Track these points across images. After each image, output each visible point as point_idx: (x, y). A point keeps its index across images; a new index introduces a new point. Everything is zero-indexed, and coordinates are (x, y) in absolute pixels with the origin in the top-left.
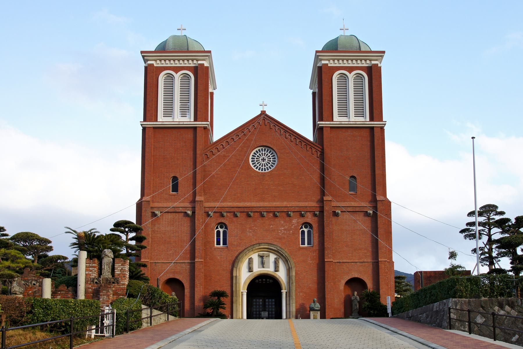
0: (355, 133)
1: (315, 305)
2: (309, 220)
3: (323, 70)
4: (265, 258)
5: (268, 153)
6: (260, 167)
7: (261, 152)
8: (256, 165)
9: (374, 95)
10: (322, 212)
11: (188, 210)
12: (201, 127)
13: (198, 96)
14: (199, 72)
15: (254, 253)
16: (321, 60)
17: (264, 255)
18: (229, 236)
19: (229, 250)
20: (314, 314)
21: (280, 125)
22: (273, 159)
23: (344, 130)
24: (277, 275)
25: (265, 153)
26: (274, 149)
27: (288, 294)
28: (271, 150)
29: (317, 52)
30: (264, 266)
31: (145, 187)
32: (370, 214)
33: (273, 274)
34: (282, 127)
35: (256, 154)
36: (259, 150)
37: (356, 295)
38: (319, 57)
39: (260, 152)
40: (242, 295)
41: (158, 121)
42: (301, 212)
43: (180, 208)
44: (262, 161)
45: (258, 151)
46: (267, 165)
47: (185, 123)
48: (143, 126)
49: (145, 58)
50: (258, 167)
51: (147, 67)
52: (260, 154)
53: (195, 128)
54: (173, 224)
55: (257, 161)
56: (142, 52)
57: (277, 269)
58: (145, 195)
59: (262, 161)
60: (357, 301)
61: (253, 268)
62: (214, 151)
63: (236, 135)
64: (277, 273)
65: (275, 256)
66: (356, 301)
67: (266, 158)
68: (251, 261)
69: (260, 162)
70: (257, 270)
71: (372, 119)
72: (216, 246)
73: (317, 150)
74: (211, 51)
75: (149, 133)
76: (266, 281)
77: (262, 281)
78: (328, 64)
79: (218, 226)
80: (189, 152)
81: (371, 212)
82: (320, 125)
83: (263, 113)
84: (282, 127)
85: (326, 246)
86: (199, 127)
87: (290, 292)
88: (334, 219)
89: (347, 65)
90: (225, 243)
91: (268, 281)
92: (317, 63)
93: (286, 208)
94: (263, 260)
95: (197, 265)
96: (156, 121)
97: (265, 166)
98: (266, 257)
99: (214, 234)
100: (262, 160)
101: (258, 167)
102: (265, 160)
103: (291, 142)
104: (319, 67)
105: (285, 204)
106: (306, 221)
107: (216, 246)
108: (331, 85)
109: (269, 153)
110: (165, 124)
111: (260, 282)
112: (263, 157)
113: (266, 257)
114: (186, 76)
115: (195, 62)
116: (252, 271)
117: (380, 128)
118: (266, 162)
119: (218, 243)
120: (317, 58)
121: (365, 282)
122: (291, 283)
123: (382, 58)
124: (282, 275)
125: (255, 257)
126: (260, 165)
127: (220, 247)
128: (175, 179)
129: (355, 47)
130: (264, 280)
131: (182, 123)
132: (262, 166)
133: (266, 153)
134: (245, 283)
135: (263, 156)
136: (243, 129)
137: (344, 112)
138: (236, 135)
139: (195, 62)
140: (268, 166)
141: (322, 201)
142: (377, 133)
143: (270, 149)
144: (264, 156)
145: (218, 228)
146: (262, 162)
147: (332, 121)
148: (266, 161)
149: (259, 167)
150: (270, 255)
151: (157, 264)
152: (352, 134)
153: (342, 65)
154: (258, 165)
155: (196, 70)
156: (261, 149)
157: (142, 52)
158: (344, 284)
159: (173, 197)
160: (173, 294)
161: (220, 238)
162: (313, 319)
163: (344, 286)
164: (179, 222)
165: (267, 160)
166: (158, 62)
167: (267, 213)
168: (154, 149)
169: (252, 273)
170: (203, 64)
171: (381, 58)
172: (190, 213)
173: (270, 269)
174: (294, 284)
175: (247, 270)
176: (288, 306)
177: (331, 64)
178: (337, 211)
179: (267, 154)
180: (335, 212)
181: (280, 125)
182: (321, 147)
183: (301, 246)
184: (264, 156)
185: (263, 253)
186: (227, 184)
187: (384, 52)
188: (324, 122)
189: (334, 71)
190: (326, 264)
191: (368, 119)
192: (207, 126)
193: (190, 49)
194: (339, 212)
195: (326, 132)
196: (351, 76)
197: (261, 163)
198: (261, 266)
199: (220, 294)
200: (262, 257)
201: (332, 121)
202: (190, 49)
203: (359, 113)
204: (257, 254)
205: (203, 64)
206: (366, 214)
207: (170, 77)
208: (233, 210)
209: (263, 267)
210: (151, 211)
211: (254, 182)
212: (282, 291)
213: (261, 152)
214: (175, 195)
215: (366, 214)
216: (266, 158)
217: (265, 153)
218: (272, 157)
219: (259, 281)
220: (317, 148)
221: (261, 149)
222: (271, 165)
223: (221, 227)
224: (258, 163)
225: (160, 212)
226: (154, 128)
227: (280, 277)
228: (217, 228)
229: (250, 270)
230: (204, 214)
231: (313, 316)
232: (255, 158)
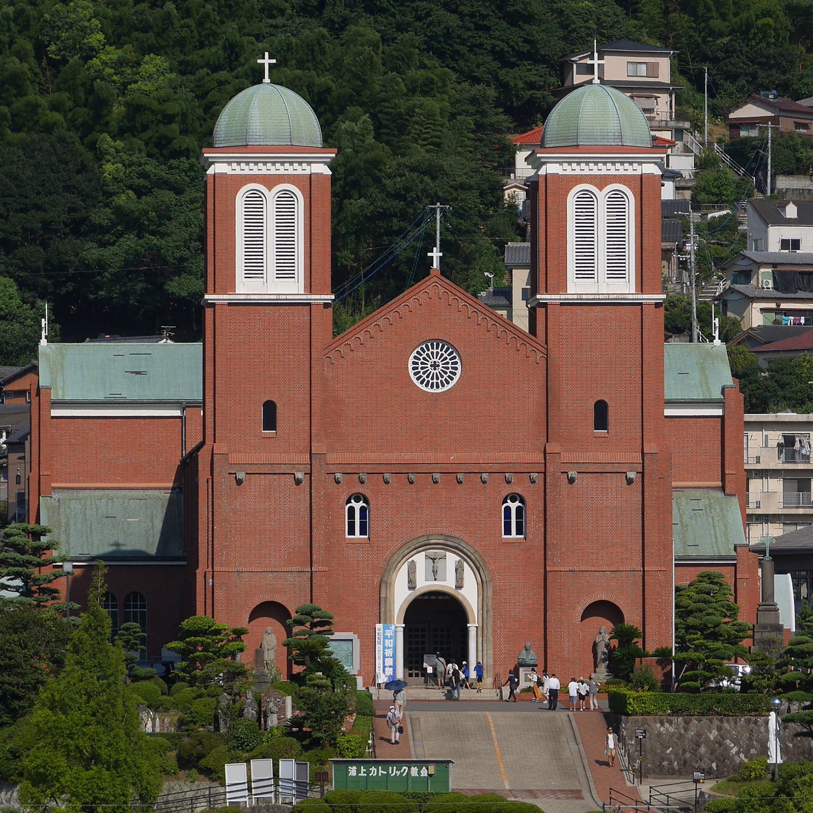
6: (428, 381)
47: (288, 297)
50: (424, 379)
57: (459, 587)
61: (415, 581)
65: (458, 558)
70: (424, 584)
124: (470, 595)
131: (284, 297)
146: (433, 371)
149: (427, 379)
154: (425, 376)
173: (447, 583)
209: (435, 580)
212: (468, 625)
229: (412, 586)
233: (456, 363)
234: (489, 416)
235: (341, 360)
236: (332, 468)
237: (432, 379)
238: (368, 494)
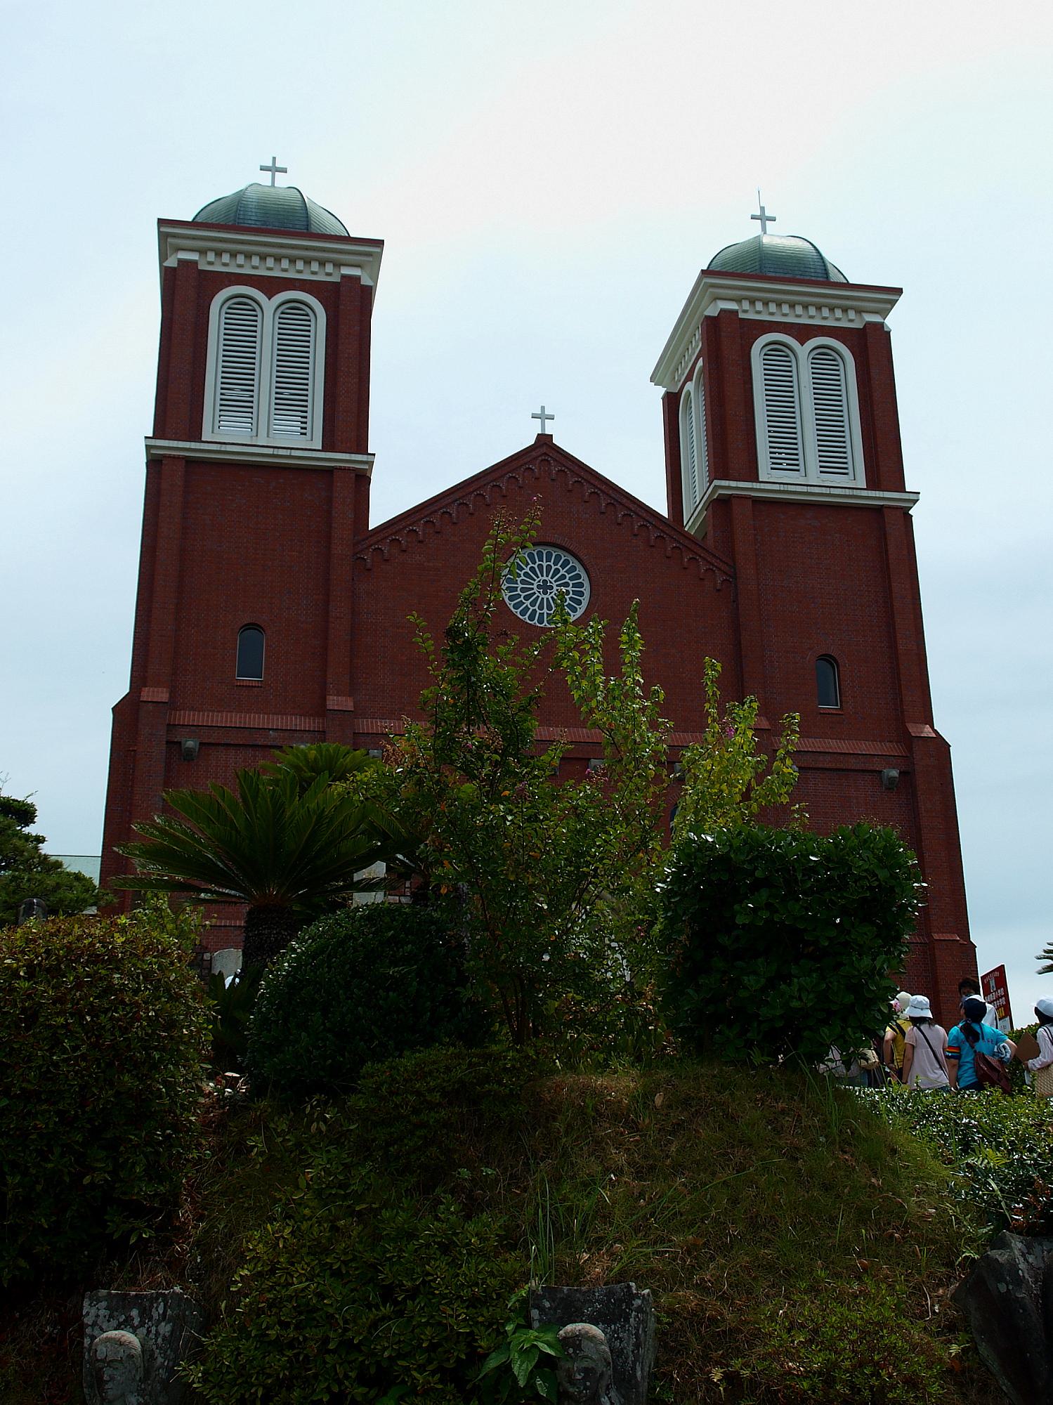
7: (538, 563)
29: (702, 270)
34: (603, 488)
47: (294, 453)
48: (153, 451)
51: (175, 268)
53: (329, 472)
55: (523, 590)
56: (161, 222)
67: (553, 581)
71: (873, 483)
78: (736, 312)
82: (721, 492)
83: (544, 441)
89: (791, 319)
101: (527, 608)
104: (708, 318)
126: (533, 604)
129: (812, 270)
131: (287, 452)
133: (554, 568)
137: (789, 458)
139: (329, 268)
143: (566, 554)
144: (547, 576)
147: (756, 480)
153: (778, 318)
157: (161, 222)
177: (749, 312)
179: (557, 571)
184: (547, 576)
187: (899, 291)
192: (366, 467)
201: (756, 480)
202: (314, 229)
203: (832, 460)
205: (358, 278)
213: (538, 563)
216: (553, 581)
233: (581, 585)
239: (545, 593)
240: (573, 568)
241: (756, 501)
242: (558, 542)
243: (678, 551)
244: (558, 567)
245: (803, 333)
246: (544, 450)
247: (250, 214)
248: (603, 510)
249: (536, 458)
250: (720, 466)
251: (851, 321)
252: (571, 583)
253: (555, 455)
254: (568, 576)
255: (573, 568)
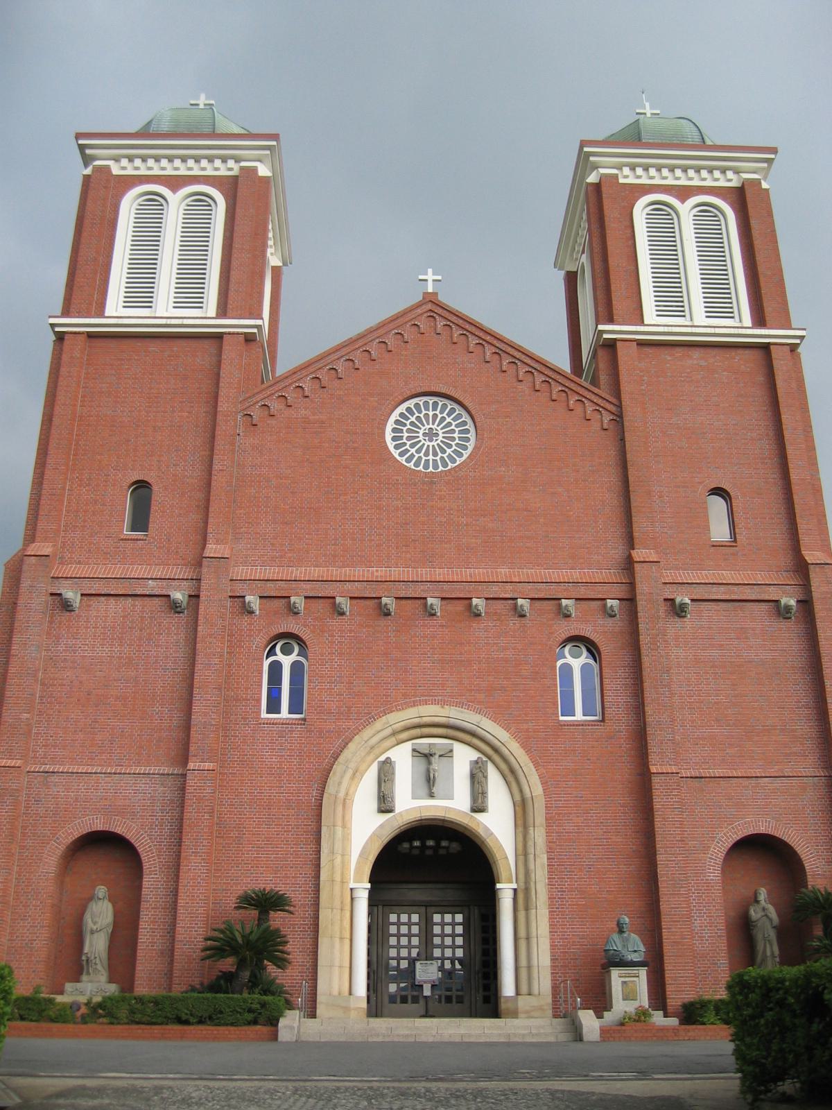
0: (711, 360)
1: (625, 941)
2: (587, 631)
3: (604, 189)
4: (435, 760)
5: (445, 415)
6: (420, 458)
7: (424, 412)
8: (407, 451)
9: (760, 258)
10: (630, 601)
11: (178, 589)
12: (238, 334)
13: (234, 250)
14: (242, 192)
15: (398, 744)
16: (595, 167)
17: (433, 751)
18: (310, 681)
19: (310, 731)
20: (627, 979)
21: (481, 334)
22: (460, 432)
23: (679, 352)
24: (479, 823)
25: (435, 416)
26: (466, 403)
27: (523, 898)
28: (456, 406)
30: (434, 790)
31: (41, 513)
32: (788, 609)
33: (465, 821)
34: (488, 338)
35: (408, 419)
36: (417, 405)
37: (763, 902)
38: (592, 159)
39: (420, 412)
40: (352, 899)
41: (106, 315)
42: (560, 599)
43: (150, 582)
44: (427, 438)
45: (414, 409)
46: (443, 451)
48: (57, 329)
49: (88, 152)
50: (412, 456)
52: (418, 418)
53: (219, 337)
54: (122, 637)
55: (409, 438)
56: (78, 136)
58: (38, 539)
59: (427, 438)
60: (772, 924)
62: (275, 406)
63: (377, 341)
64: (478, 816)
65: (474, 755)
66: (769, 927)
67: (438, 428)
68: (386, 773)
69: (420, 441)
71: (760, 319)
72: (264, 715)
73: (600, 406)
74: (278, 135)
75: (74, 350)
76: (438, 846)
77: (423, 847)
79: (274, 646)
80: (193, 407)
81: (793, 602)
82: (605, 336)
84: (488, 338)
85: (649, 720)
86: (229, 333)
87: (527, 890)
88: (674, 627)
90: (295, 707)
91: (444, 847)
92: (585, 174)
93: (509, 586)
94: (431, 767)
95: (191, 781)
96: (101, 314)
97: (435, 454)
98: (440, 756)
99: (261, 673)
100: (424, 434)
101: (412, 456)
102: (437, 435)
103: (519, 383)
105: (503, 572)
106: (577, 633)
107: (264, 715)
108: (629, 231)
109: (449, 415)
110: (172, 323)
111: (416, 852)
112: (429, 427)
113: (440, 756)
114: (202, 200)
115: (231, 163)
116: (390, 811)
117: (788, 347)
118: (439, 442)
119: (274, 706)
120: (584, 162)
121: (795, 853)
122: (531, 857)
123: (770, 167)
125: (402, 757)
126: (418, 451)
127: (278, 721)
128: (141, 487)
130: (431, 843)
132: (427, 454)
133: (440, 416)
134: (363, 854)
135: (428, 424)
136: (366, 344)
137: (673, 300)
138: (377, 341)
140: (447, 454)
141: (629, 565)
142: (780, 362)
143: (452, 403)
144: (433, 424)
145: (276, 655)
146: (427, 443)
147: (642, 323)
148: (440, 438)
149: (417, 456)
150: (455, 753)
151: (54, 778)
152: (703, 363)
153: (657, 181)
154: (413, 451)
155: (231, 187)
156: (421, 403)
158: (721, 856)
159: (130, 544)
160: (101, 895)
161: (281, 688)
162: (624, 999)
163: (723, 871)
164: (141, 630)
165: (441, 435)
166: (124, 162)
167: (445, 602)
168: (84, 396)
169: (391, 815)
170: (255, 170)
171: (765, 165)
172: (181, 598)
174: (543, 859)
175: (373, 804)
176: (523, 944)
177: (627, 177)
178: (678, 600)
179: (443, 419)
180: (673, 600)
181: (481, 334)
182: (614, 400)
183: (562, 718)
184: (433, 424)
185: (430, 744)
186: (310, 508)
188: (635, 327)
189: (636, 194)
190: (655, 780)
191: (747, 321)
192: (255, 330)
193: (218, 131)
194: (687, 600)
195: (625, 355)
196: (686, 210)
197: (424, 444)
198: (423, 790)
199: (266, 903)
200: (425, 756)
201: (642, 323)
203: (719, 304)
204: (408, 746)
206: (782, 612)
207: (155, 201)
208: (327, 590)
209: (431, 795)
210: (50, 591)
211: (399, 503)
212: (498, 886)
213: (424, 412)
214: (137, 540)
215: (782, 612)
216: (438, 428)
217: (435, 416)
218: (457, 426)
219: (412, 847)
220: (600, 401)
221: (421, 403)
222: (455, 451)
223: (286, 651)
224: (412, 446)
225: (82, 595)
226: (91, 336)
227: (492, 834)
228: (272, 652)
229: (385, 804)
230: (229, 603)
231: (620, 988)
232: (405, 429)
233: (467, 431)
234: (526, 510)
235: (272, 422)
236: (239, 589)
237: (427, 454)
238: (305, 634)
239: (431, 440)
240: (460, 416)
241: (641, 344)
242: (443, 391)
243: (564, 395)
244: (445, 415)
245: (684, 193)
246: (429, 306)
247: (163, 126)
248: (504, 369)
249: (422, 314)
250: (607, 313)
251: (730, 180)
252: (457, 430)
253: (440, 311)
254: (454, 423)
255: (460, 416)
